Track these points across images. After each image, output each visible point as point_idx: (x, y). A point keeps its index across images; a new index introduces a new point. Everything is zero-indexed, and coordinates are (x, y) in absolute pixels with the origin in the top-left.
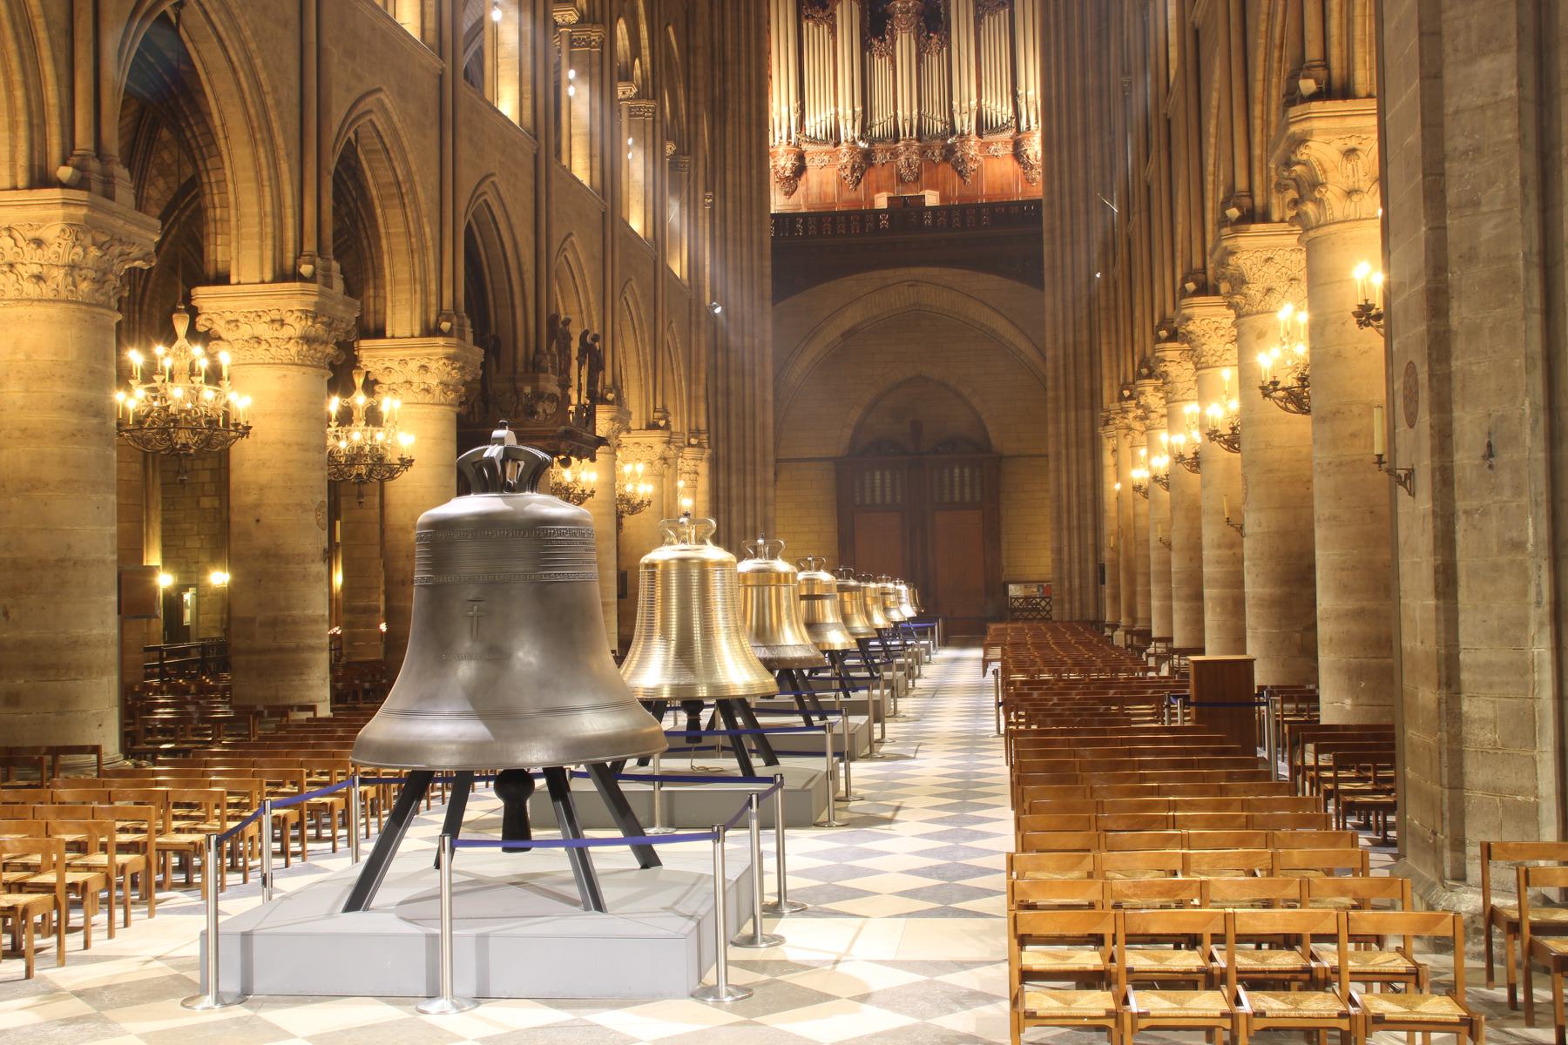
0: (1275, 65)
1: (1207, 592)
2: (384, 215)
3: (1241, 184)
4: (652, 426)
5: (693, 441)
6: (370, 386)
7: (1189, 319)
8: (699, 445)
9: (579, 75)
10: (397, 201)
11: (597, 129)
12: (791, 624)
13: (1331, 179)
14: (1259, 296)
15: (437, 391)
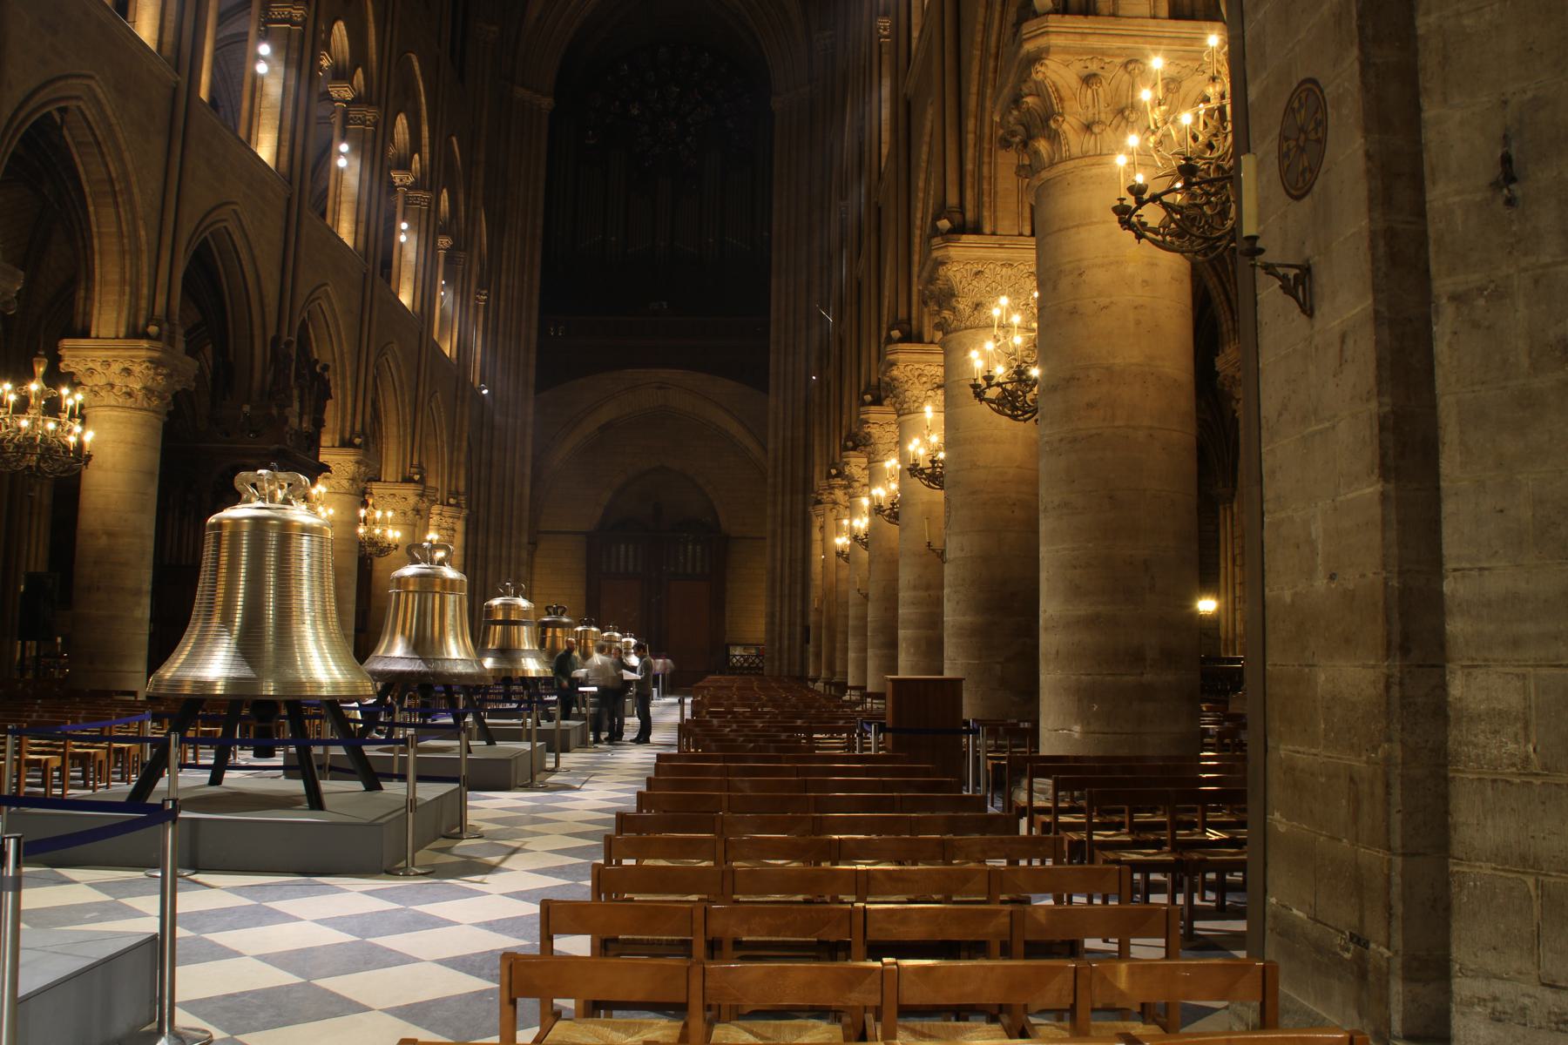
0: (991, 75)
1: (901, 633)
2: (96, 213)
3: (952, 199)
4: (407, 480)
5: (452, 501)
6: (55, 377)
7: (893, 364)
8: (457, 505)
9: (352, 150)
10: (110, 200)
11: (365, 198)
12: (456, 637)
13: (1067, 109)
14: (968, 311)
15: (140, 395)
